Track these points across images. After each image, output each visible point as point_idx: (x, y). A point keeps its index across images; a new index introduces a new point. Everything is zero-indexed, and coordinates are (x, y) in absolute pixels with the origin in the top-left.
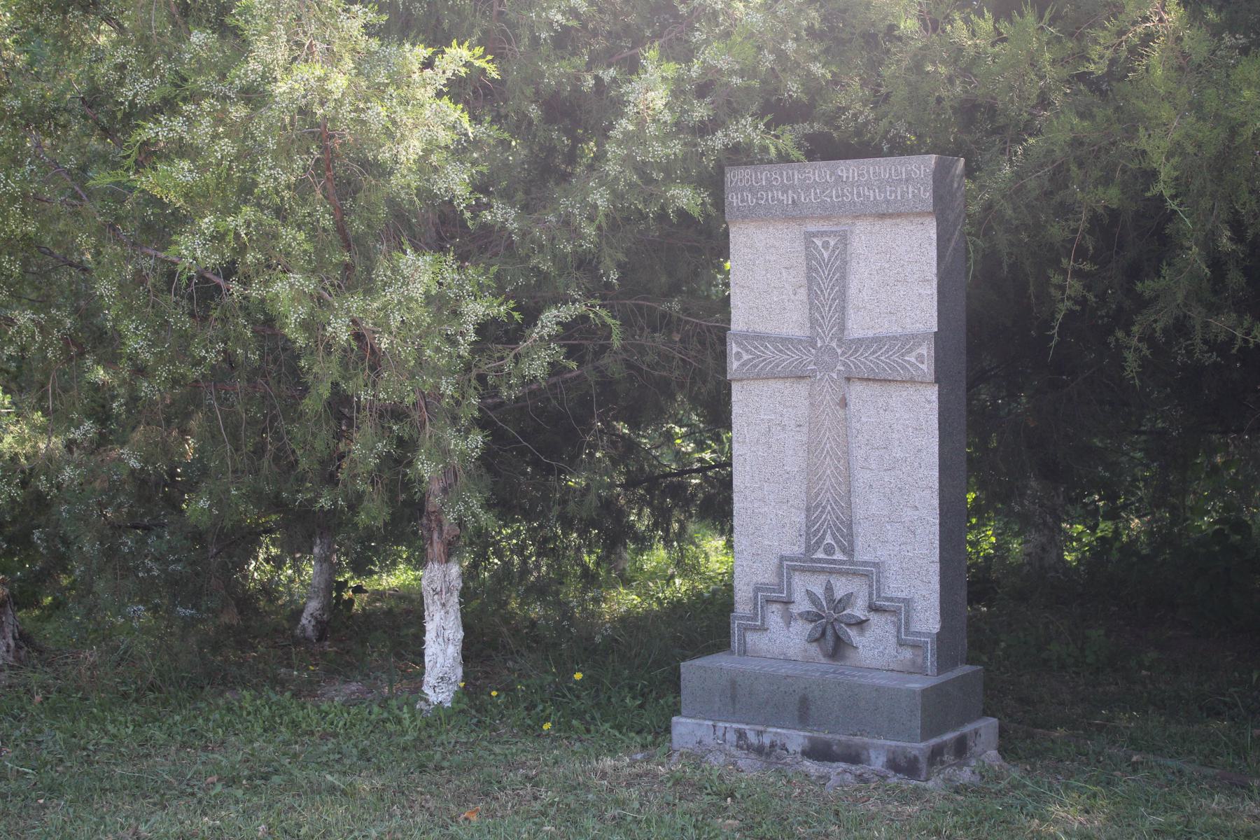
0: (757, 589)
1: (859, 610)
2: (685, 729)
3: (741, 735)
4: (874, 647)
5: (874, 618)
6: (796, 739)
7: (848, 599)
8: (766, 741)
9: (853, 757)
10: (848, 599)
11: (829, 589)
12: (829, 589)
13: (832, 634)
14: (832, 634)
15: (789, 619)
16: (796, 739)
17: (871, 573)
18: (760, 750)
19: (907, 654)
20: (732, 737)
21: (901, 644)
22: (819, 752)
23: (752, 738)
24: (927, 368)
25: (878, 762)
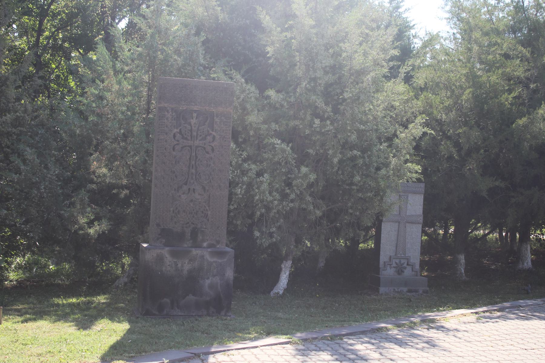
0: (384, 262)
1: (405, 265)
2: (382, 290)
3: (394, 289)
4: (408, 272)
5: (408, 266)
6: (405, 289)
7: (403, 264)
8: (399, 290)
9: (416, 291)
10: (403, 264)
11: (400, 262)
12: (400, 262)
13: (400, 270)
14: (400, 270)
15: (391, 268)
16: (405, 289)
17: (408, 259)
18: (398, 292)
19: (413, 273)
20: (392, 290)
21: (412, 271)
22: (410, 291)
23: (396, 290)
24: (421, 221)
25: (421, 292)
